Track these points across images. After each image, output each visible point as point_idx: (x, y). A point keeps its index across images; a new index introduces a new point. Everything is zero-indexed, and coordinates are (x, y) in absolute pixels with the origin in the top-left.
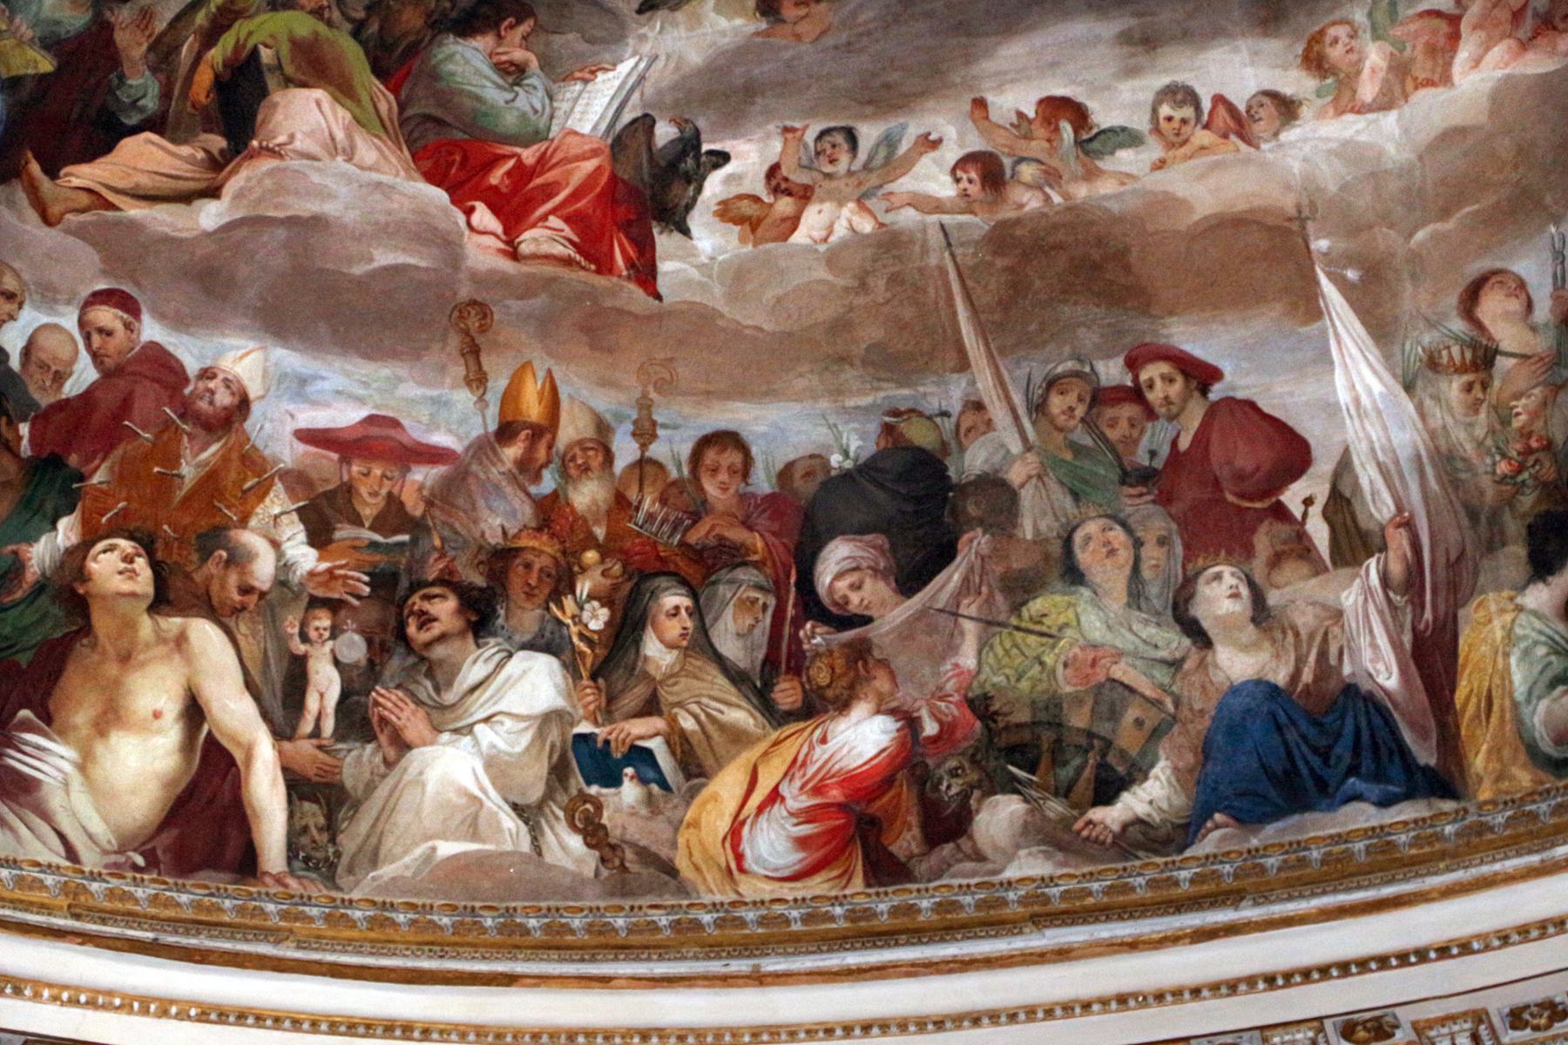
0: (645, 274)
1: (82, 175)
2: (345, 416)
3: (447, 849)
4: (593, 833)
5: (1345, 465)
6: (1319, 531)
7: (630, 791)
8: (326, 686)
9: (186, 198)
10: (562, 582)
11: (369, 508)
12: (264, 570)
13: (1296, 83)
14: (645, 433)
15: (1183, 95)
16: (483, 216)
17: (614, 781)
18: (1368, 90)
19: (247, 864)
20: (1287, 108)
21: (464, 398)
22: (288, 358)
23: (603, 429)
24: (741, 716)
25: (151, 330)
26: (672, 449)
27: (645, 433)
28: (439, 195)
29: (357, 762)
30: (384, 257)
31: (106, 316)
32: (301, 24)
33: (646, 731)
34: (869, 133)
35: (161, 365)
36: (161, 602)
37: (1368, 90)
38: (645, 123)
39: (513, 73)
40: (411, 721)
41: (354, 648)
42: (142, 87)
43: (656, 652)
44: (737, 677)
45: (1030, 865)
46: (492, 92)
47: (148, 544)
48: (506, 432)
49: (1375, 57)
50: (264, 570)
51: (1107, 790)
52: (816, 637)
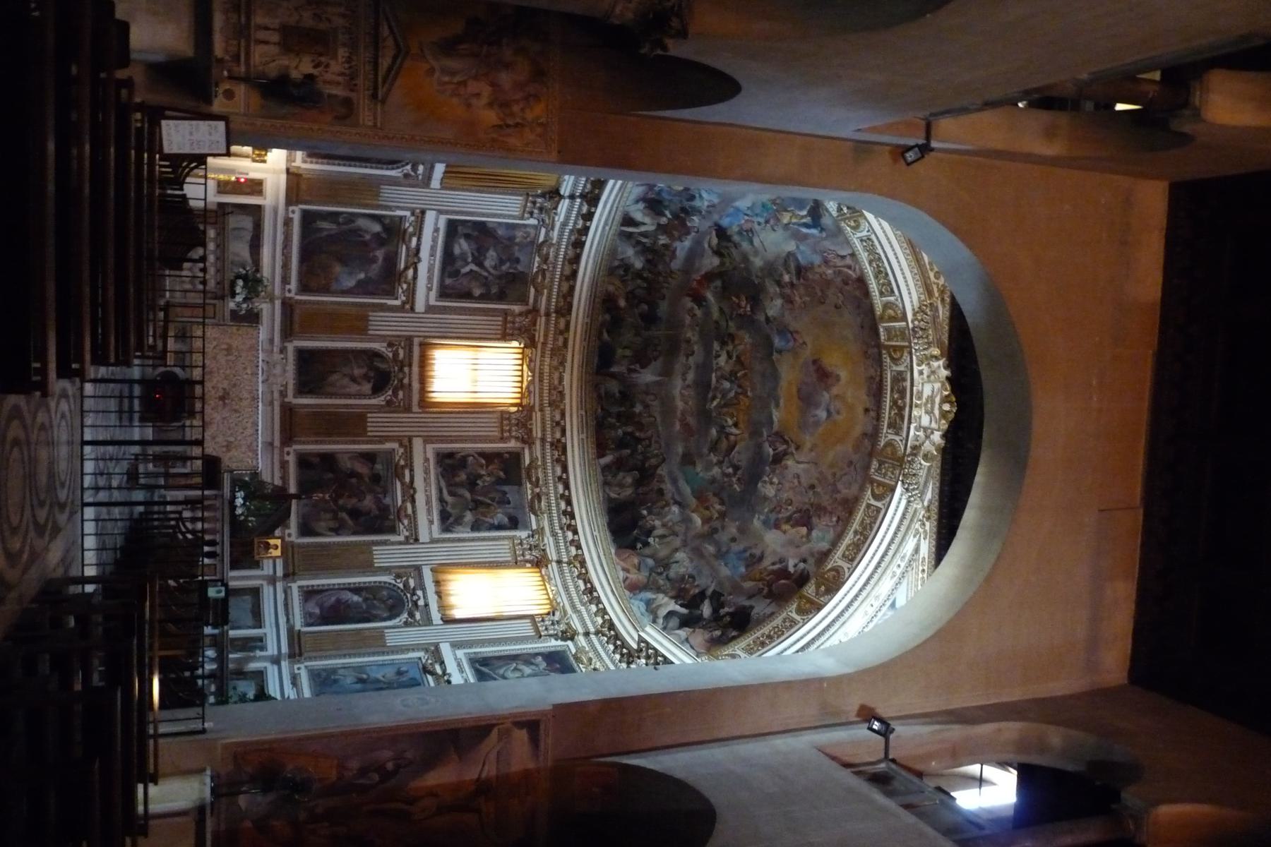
0: (689, 295)
1: (714, 233)
2: (678, 253)
3: (620, 249)
4: (618, 267)
5: (639, 373)
6: (633, 367)
7: (622, 273)
8: (644, 240)
9: (709, 246)
10: (650, 272)
11: (667, 252)
12: (660, 237)
13: (687, 382)
14: (667, 288)
15: (690, 368)
16: (699, 278)
17: (624, 271)
18: (683, 391)
19: (623, 225)
20: (684, 380)
21: (677, 267)
22: (686, 249)
23: (668, 283)
24: (629, 288)
25: (693, 234)
26: (664, 291)
27: (667, 288)
28: (703, 273)
29: (633, 242)
30: (697, 264)
31: (696, 230)
32: (728, 264)
33: (629, 277)
34: (697, 328)
35: (688, 233)
36: (659, 225)
37: (683, 391)
38: (706, 301)
39: (716, 288)
40: (636, 249)
41: (648, 245)
42: (725, 244)
43: (639, 281)
44: (633, 290)
45: (600, 318)
46: (714, 284)
47: (666, 225)
48: (671, 272)
49: (687, 393)
50: (660, 237)
51: (608, 332)
52: (636, 301)
